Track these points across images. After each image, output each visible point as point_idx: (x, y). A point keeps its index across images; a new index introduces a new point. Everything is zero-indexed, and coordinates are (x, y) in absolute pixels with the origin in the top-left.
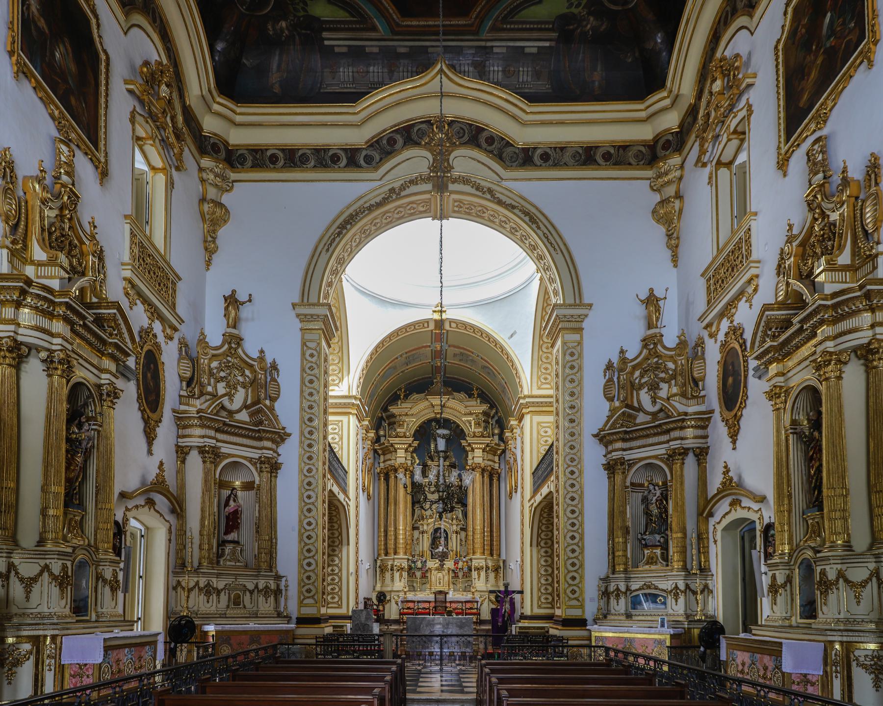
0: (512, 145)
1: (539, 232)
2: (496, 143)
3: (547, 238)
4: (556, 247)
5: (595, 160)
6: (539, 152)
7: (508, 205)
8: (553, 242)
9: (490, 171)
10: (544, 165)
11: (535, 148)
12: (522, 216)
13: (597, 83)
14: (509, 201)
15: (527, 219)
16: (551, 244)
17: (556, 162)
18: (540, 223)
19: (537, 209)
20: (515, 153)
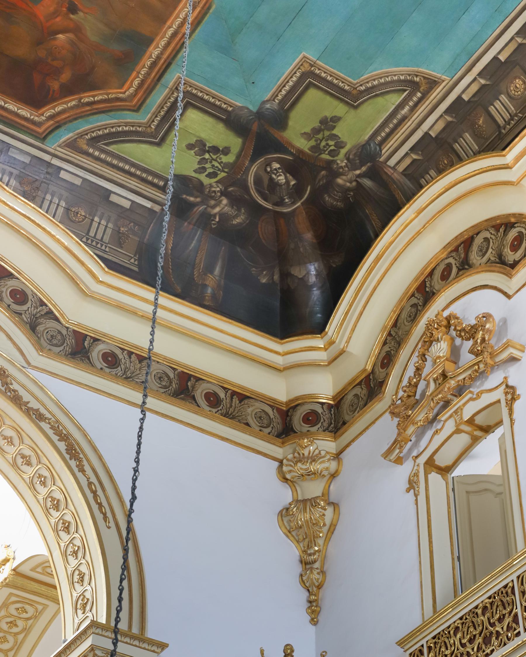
0: (57, 319)
1: (80, 475)
2: (29, 304)
3: (94, 493)
4: (109, 514)
5: (194, 398)
6: (101, 348)
7: (32, 408)
8: (105, 503)
9: (9, 343)
10: (108, 370)
11: (96, 340)
12: (55, 438)
13: (209, 290)
14: (34, 404)
15: (62, 446)
16: (100, 505)
17: (129, 374)
18: (85, 462)
19: (85, 435)
20: (60, 332)
